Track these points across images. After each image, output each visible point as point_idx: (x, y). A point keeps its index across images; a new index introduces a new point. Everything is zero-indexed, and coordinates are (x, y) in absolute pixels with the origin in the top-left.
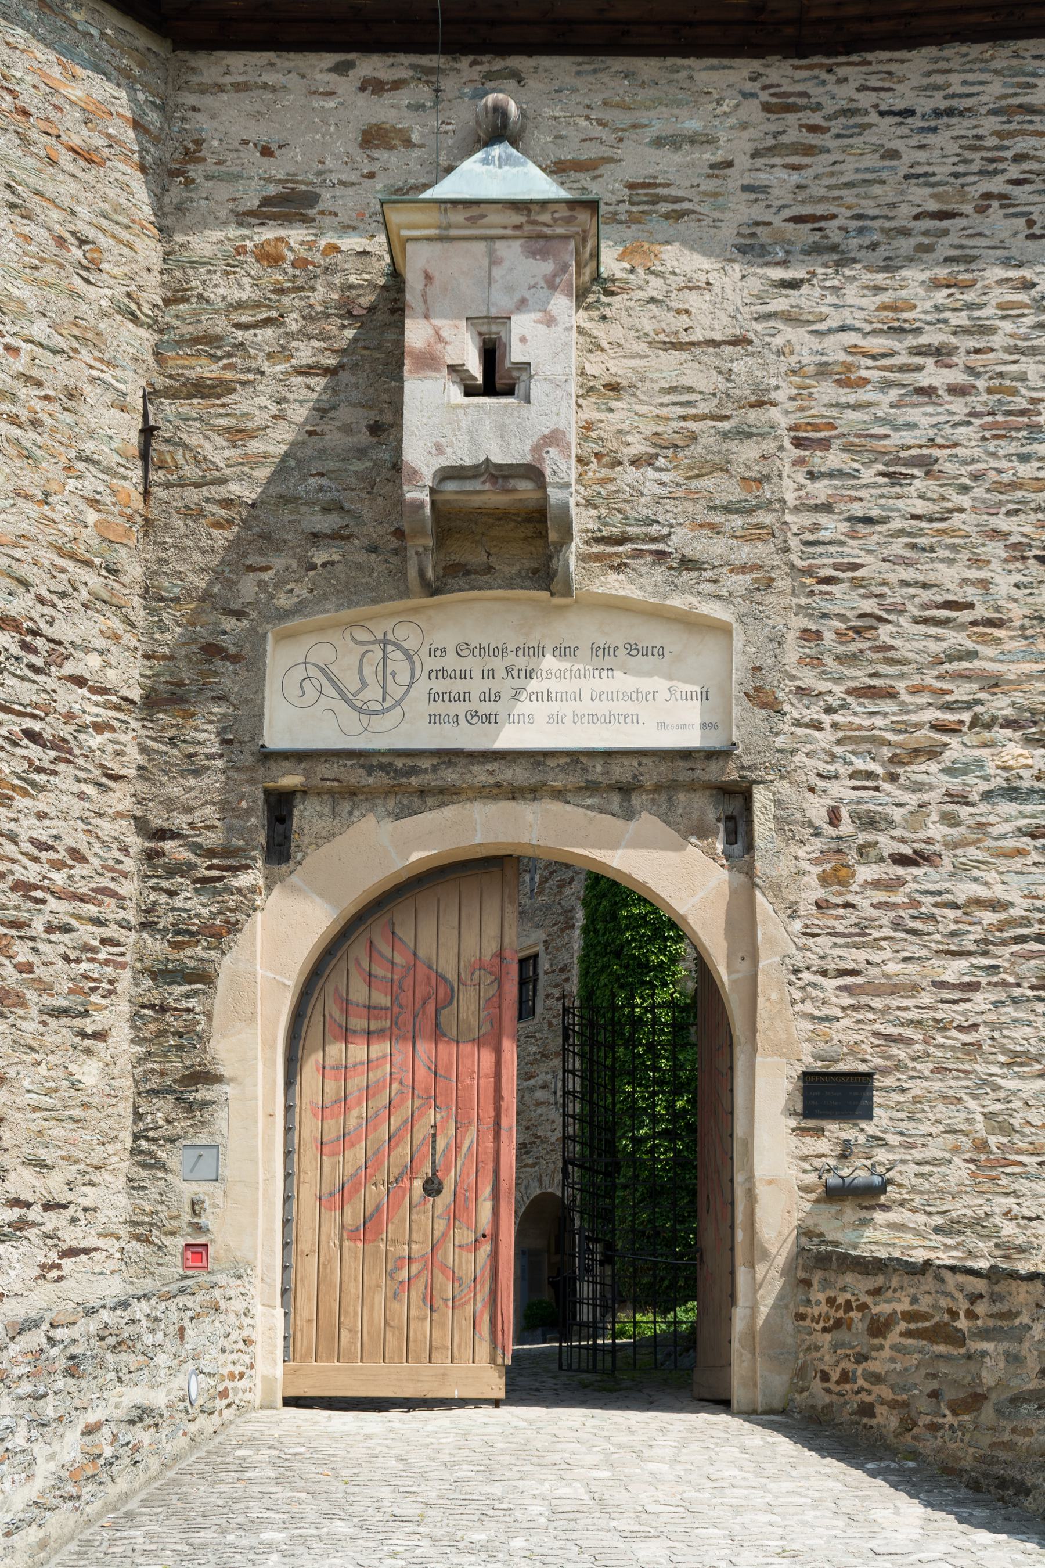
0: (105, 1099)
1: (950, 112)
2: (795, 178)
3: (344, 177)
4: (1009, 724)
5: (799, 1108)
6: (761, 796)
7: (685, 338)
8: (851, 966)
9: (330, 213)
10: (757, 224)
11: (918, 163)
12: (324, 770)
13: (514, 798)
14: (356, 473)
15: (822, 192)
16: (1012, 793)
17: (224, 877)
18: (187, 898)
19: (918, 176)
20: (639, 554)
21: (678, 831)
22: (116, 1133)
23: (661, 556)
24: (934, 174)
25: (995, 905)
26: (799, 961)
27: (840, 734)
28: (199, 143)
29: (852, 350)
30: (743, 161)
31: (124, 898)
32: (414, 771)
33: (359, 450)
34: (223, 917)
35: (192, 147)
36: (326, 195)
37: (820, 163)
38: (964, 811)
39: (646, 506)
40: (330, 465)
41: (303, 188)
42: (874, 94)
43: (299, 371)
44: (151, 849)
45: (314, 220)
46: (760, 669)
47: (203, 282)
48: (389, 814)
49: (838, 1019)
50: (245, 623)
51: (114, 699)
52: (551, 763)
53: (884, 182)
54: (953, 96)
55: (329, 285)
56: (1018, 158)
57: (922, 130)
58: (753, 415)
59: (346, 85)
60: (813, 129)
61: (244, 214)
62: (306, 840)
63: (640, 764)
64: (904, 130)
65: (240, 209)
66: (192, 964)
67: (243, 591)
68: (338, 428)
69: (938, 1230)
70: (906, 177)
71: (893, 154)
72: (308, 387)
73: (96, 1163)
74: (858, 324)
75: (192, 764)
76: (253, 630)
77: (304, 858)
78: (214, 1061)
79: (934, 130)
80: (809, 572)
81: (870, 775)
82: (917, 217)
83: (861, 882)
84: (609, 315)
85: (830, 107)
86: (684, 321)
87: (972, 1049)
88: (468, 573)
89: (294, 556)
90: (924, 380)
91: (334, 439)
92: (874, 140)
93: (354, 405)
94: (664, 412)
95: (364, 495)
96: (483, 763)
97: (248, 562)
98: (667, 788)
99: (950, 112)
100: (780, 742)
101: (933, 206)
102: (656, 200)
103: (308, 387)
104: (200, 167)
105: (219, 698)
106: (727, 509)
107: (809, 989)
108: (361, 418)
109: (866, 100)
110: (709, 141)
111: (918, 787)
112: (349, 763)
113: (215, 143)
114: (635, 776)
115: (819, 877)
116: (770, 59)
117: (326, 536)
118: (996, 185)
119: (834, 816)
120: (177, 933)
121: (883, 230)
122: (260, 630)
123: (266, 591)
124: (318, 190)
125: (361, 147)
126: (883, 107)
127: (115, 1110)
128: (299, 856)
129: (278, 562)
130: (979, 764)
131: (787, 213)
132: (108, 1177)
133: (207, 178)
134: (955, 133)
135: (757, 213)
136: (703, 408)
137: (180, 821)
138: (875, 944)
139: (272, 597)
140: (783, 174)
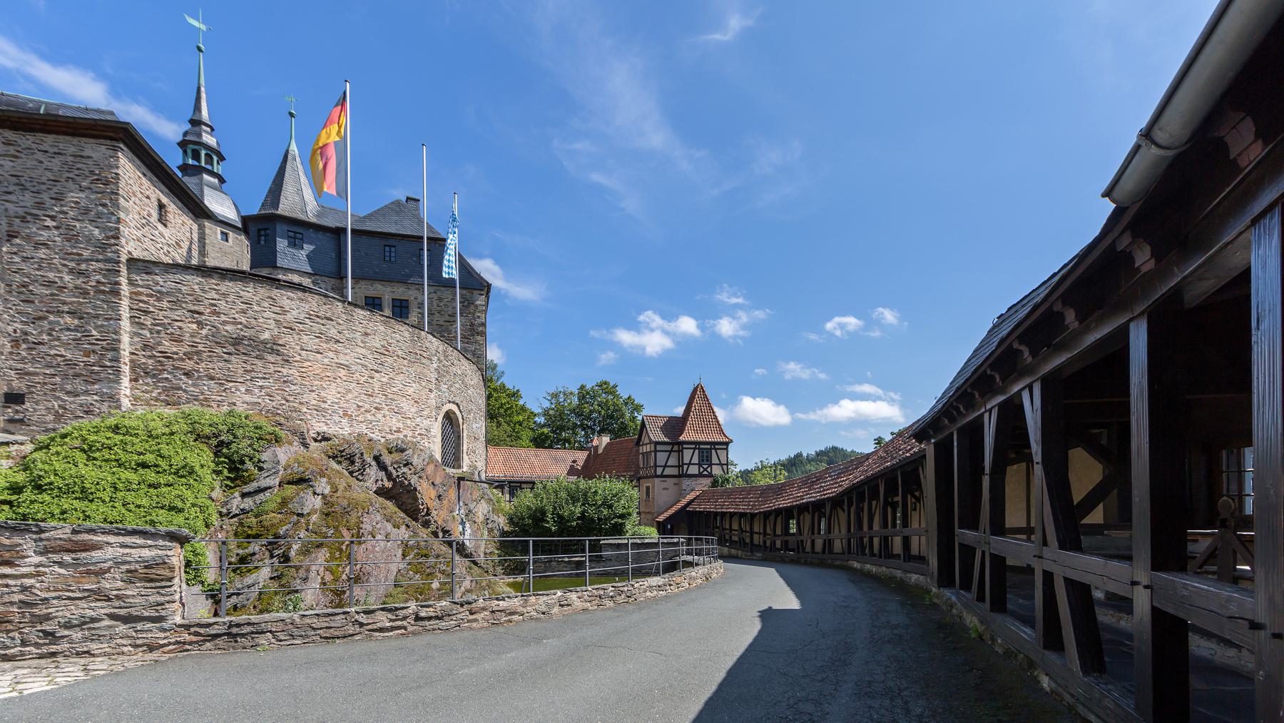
1: (59, 154)
2: (12, 164)
4: (68, 313)
15: (20, 169)
16: (68, 329)
25: (61, 356)
29: (26, 213)
37: (20, 161)
38: (54, 333)
56: (78, 169)
64: (44, 156)
69: (43, 431)
71: (41, 162)
79: (53, 157)
80: (9, 269)
81: (26, 322)
82: (48, 180)
85: (23, 146)
87: (54, 390)
92: (36, 158)
99: (59, 154)
109: (34, 146)
111: (41, 326)
116: (5, 130)
118: (71, 175)
119: (15, 331)
131: (9, 173)
138: (25, 363)
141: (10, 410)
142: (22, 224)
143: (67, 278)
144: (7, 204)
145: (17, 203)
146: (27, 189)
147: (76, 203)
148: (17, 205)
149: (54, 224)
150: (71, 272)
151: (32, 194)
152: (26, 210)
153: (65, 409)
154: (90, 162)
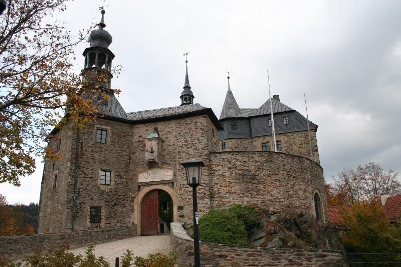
6: (175, 183)
59: (144, 126)
98: (168, 183)
110: (172, 127)
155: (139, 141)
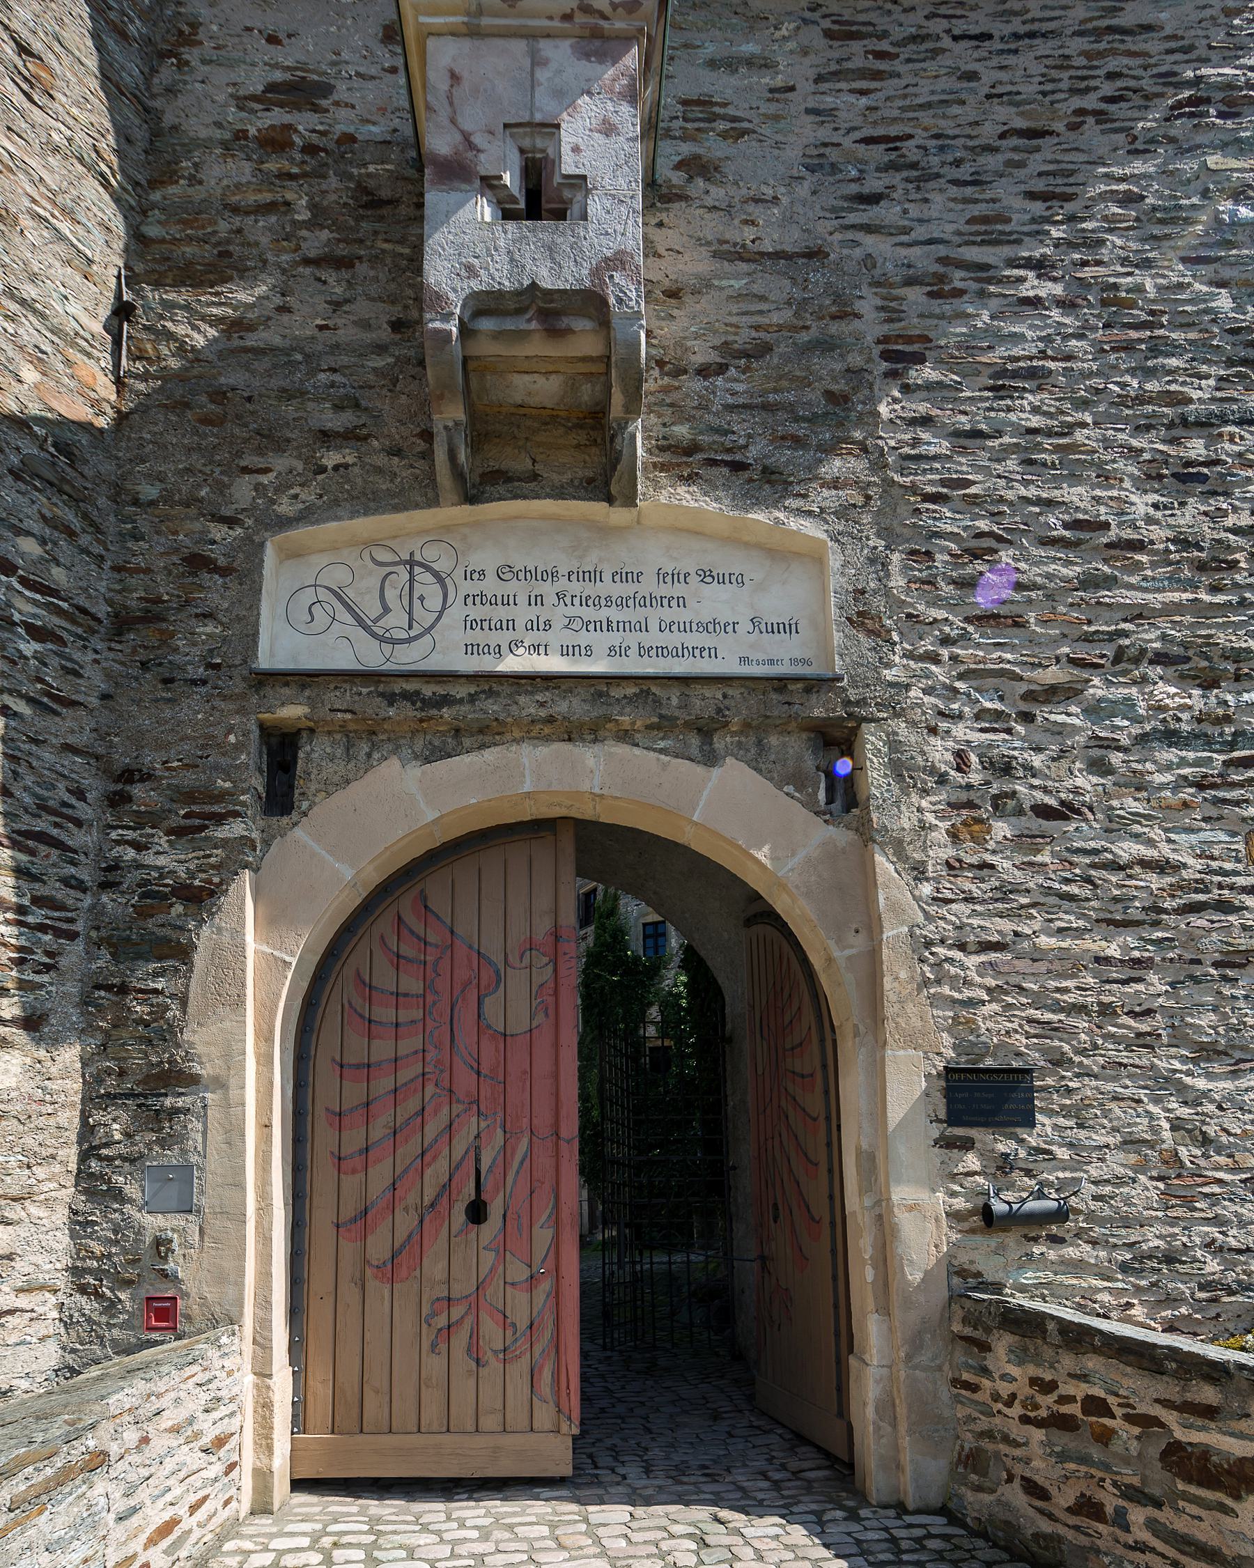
0: (34, 1106)
1: (1031, 35)
3: (362, 70)
4: (1160, 659)
5: (942, 1114)
7: (756, 247)
8: (995, 938)
9: (347, 105)
10: (825, 145)
11: (1001, 83)
12: (334, 698)
13: (570, 740)
14: (374, 369)
15: (896, 113)
16: (1171, 737)
17: (207, 827)
18: (158, 853)
19: (1000, 96)
20: (712, 463)
21: (771, 779)
22: (51, 1151)
23: (738, 467)
24: (1019, 93)
25: (1162, 867)
26: (930, 931)
27: (962, 668)
28: (195, 26)
29: (944, 261)
30: (804, 87)
31: (75, 852)
32: (446, 701)
33: (378, 346)
34: (203, 876)
35: (186, 29)
36: (341, 87)
38: (1116, 758)
39: (716, 414)
40: (344, 360)
41: (316, 77)
42: (945, 21)
43: (307, 262)
44: (115, 793)
45: (327, 111)
46: (863, 592)
47: (196, 165)
48: (416, 757)
49: (983, 1002)
50: (239, 531)
51: (65, 605)
52: (616, 693)
53: (964, 103)
54: (1033, 20)
55: (345, 176)
56: (1111, 76)
57: (1002, 52)
58: (834, 328)
60: (880, 55)
61: (246, 98)
62: (313, 787)
63: (725, 696)
65: (241, 93)
66: (161, 932)
67: (237, 495)
68: (354, 323)
70: (988, 97)
71: (972, 76)
72: (319, 280)
73: (15, 1191)
74: (946, 237)
75: (169, 690)
76: (248, 539)
77: (310, 808)
78: (188, 1057)
79: (1016, 52)
81: (998, 715)
83: (1000, 838)
84: (666, 221)
85: (898, 33)
86: (749, 233)
88: (509, 480)
89: (299, 457)
90: (1026, 291)
91: (347, 333)
92: (949, 62)
93: (373, 300)
94: (734, 320)
95: (385, 392)
96: (532, 693)
97: (243, 463)
99: (1031, 35)
100: (889, 674)
101: (1020, 123)
102: (713, 118)
103: (319, 280)
104: (196, 51)
105: (205, 616)
106: (811, 420)
107: (946, 966)
108: (382, 314)
109: (937, 26)
110: (766, 64)
111: (1060, 731)
112: (365, 691)
113: (215, 28)
114: (719, 711)
115: (948, 832)
117: (338, 434)
118: (1091, 102)
120: (144, 896)
121: (966, 147)
122: (257, 539)
123: (265, 496)
124: (332, 82)
125: (382, 41)
126: (956, 32)
127: (52, 1121)
128: (305, 805)
129: (281, 463)
130: (1129, 702)
131: (857, 135)
132: (34, 1210)
133: (204, 62)
134: (1039, 54)
135: (824, 134)
136: (775, 318)
137: (151, 759)
139: (273, 502)
140: (852, 99)
141: (972, 1161)
142: (936, 306)
143: (1141, 504)
144: (869, 240)
145: (906, 231)
146: (938, 176)
147: (1129, 199)
148: (904, 238)
149: (1058, 289)
150: (1151, 477)
151: (954, 191)
152: (942, 251)
153: (1206, 1141)
154: (1153, 45)
155: (276, 141)
